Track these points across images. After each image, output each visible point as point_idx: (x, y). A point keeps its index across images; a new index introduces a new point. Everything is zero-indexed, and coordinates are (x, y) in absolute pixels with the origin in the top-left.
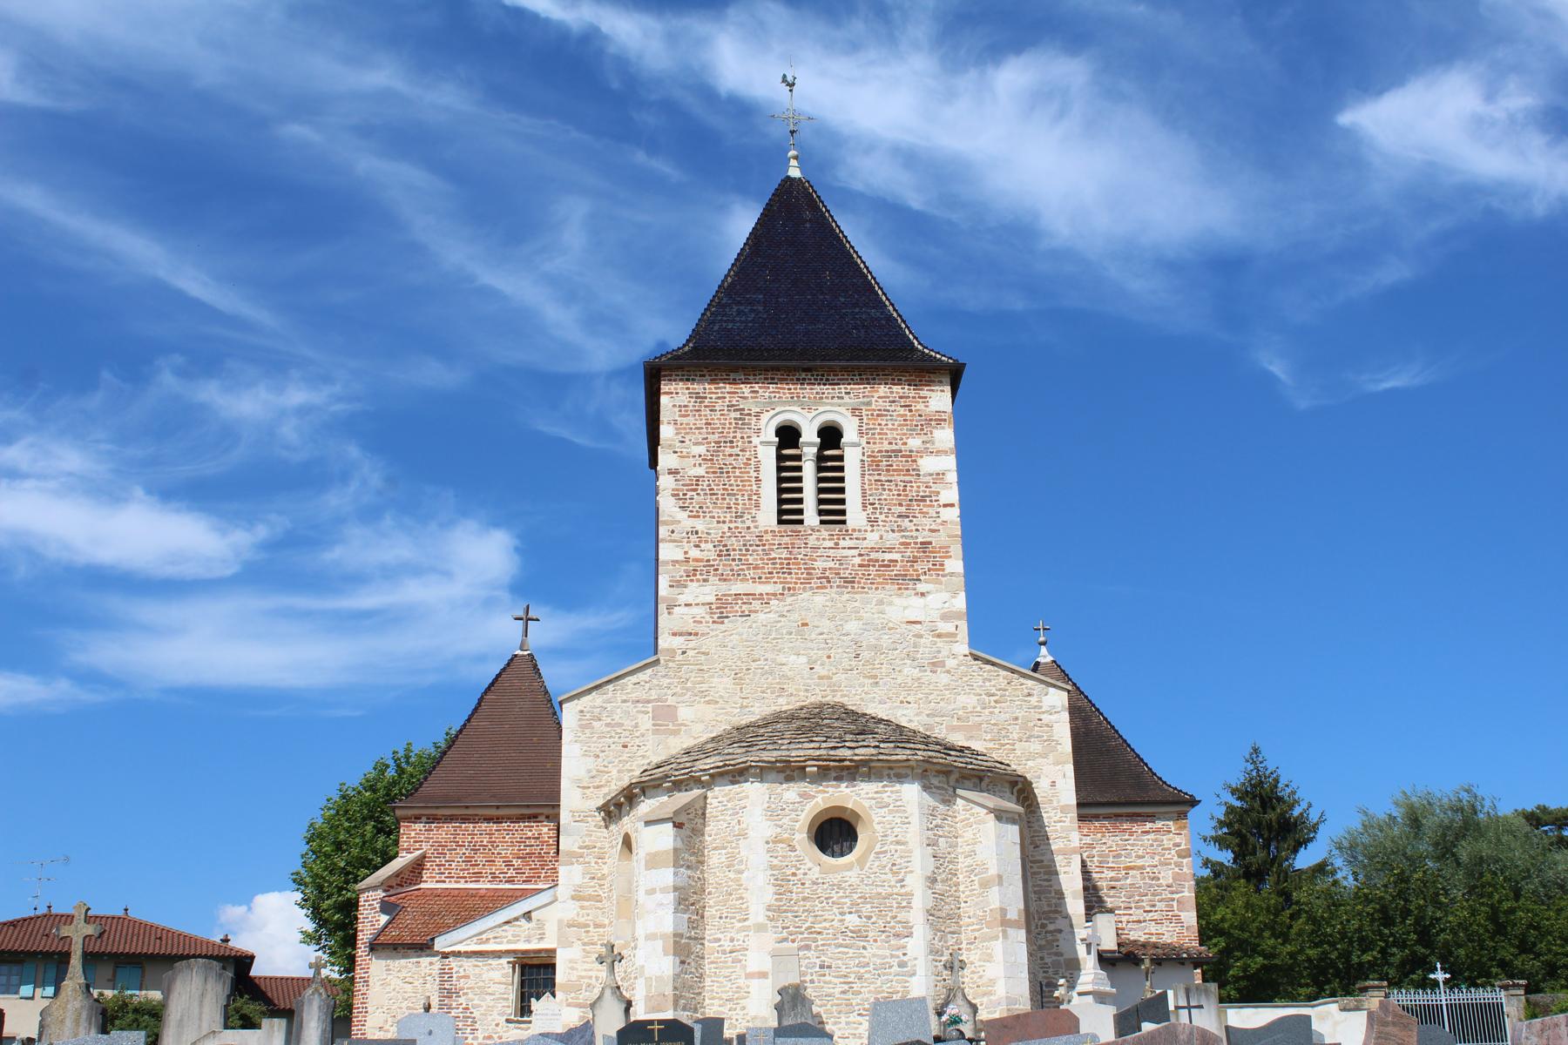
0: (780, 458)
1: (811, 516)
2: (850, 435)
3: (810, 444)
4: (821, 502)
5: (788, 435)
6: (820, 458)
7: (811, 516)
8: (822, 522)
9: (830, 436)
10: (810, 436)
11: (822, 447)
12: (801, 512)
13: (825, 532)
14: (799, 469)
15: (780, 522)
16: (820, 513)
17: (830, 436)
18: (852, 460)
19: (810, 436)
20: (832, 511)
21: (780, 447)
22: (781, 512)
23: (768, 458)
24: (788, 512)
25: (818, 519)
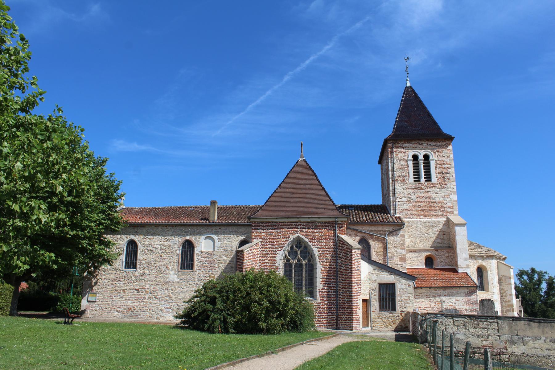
1: (423, 180)
3: (421, 160)
5: (415, 157)
7: (423, 180)
9: (426, 157)
10: (421, 157)
11: (424, 160)
13: (426, 183)
17: (426, 157)
18: (433, 164)
19: (421, 157)
20: (428, 178)
23: (411, 164)
24: (417, 179)
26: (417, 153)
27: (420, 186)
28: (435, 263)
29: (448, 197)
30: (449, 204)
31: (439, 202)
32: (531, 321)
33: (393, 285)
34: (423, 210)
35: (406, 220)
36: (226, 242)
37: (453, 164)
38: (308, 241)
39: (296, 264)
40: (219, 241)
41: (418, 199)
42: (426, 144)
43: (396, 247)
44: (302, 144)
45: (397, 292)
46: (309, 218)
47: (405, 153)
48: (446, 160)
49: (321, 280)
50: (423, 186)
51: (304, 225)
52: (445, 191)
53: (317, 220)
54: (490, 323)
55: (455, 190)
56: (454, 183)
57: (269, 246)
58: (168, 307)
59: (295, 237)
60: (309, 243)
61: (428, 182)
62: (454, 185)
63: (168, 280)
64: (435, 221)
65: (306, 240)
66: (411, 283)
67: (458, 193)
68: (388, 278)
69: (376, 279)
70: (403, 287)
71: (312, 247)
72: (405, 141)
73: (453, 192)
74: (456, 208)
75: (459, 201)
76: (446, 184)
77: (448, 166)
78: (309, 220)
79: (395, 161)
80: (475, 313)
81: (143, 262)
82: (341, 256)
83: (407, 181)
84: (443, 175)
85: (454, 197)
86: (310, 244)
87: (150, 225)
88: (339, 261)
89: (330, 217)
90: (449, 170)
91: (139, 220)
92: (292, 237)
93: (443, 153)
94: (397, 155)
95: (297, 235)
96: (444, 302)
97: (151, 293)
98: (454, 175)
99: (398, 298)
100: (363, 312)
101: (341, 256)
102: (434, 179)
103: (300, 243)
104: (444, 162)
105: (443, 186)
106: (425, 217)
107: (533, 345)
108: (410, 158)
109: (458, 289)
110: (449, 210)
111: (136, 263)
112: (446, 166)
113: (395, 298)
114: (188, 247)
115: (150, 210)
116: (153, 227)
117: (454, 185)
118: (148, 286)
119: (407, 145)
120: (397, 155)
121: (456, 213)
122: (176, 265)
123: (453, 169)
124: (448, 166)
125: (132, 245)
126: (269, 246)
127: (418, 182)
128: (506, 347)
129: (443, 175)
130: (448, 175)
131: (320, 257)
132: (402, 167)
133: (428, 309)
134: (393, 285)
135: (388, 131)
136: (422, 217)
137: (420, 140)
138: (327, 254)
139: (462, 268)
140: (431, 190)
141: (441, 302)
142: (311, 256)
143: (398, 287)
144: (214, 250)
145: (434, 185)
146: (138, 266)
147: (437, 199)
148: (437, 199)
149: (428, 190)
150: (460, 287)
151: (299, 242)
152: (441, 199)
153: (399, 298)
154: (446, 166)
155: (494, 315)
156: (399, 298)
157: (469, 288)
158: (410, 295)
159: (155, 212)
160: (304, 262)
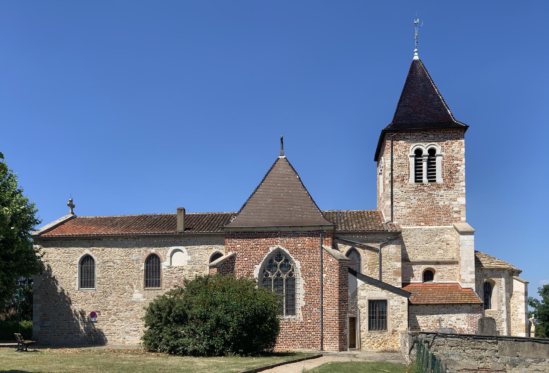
0: (416, 160)
1: (425, 180)
2: (438, 152)
4: (428, 174)
5: (418, 153)
6: (429, 160)
7: (425, 180)
8: (429, 181)
9: (432, 152)
10: (425, 152)
11: (429, 156)
12: (422, 178)
13: (430, 184)
14: (422, 164)
15: (416, 181)
16: (428, 178)
17: (432, 152)
18: (439, 160)
19: (425, 152)
20: (432, 177)
21: (416, 157)
22: (416, 178)
23: (412, 161)
24: (418, 178)
25: (427, 180)
26: (421, 147)
27: (422, 187)
28: (435, 277)
29: (455, 200)
30: (456, 209)
31: (444, 206)
32: (536, 342)
33: (385, 302)
34: (425, 216)
35: (403, 227)
36: (197, 255)
37: (464, 160)
38: (289, 253)
39: (275, 280)
40: (190, 254)
41: (419, 203)
42: (432, 136)
43: (390, 259)
44: (282, 139)
45: (389, 310)
46: (290, 227)
47: (406, 147)
48: (455, 156)
49: (304, 297)
50: (425, 188)
51: (285, 235)
52: (451, 194)
53: (300, 229)
54: (490, 343)
55: (464, 191)
56: (464, 184)
57: (246, 259)
58: (135, 329)
59: (275, 248)
60: (290, 255)
61: (433, 183)
62: (463, 186)
63: (132, 300)
64: (438, 229)
65: (287, 251)
66: (405, 299)
67: (468, 195)
68: (379, 294)
69: (366, 295)
70: (396, 303)
71: (294, 260)
72: (407, 132)
73: (462, 194)
74: (463, 213)
75: (468, 205)
76: (454, 185)
77: (458, 162)
78: (291, 230)
79: (394, 157)
80: (473, 333)
81: (102, 280)
82: (326, 269)
83: (406, 182)
84: (451, 174)
85: (462, 200)
86: (292, 257)
87: (108, 237)
88: (324, 275)
89: (314, 226)
90: (458, 168)
91: (95, 231)
92: (271, 249)
93: (453, 147)
94: (396, 150)
95: (277, 246)
96: (442, 320)
97: (115, 314)
98: (464, 174)
99: (389, 316)
100: (350, 331)
101: (326, 269)
102: (439, 179)
103: (280, 255)
104: (453, 158)
105: (449, 188)
106: (426, 224)
107: (536, 367)
108: (413, 153)
109: (460, 305)
110: (455, 215)
111: (94, 282)
112: (455, 162)
113: (386, 317)
114: (153, 263)
115: (106, 219)
116: (111, 239)
117: (463, 186)
118: (109, 307)
119: (409, 137)
120: (396, 150)
121: (463, 219)
122: (142, 282)
123: (464, 166)
124: (458, 162)
125: (87, 260)
126: (246, 259)
127: (421, 183)
128: (505, 369)
129: (451, 174)
130: (457, 174)
131: (302, 270)
132: (401, 165)
133: (424, 328)
134: (385, 302)
135: (387, 120)
136: (422, 224)
137: (426, 131)
138: (311, 268)
139: (467, 282)
140: (435, 193)
141: (440, 321)
142: (293, 270)
143: (391, 303)
144: (184, 263)
145: (439, 187)
146: (96, 285)
147: (441, 203)
148: (441, 203)
149: (431, 192)
150: (461, 304)
151: (279, 254)
152: (447, 203)
153: (391, 316)
154: (455, 162)
155: (494, 335)
156: (391, 316)
157: (473, 305)
158: (402, 313)
159: (111, 222)
160: (284, 277)
